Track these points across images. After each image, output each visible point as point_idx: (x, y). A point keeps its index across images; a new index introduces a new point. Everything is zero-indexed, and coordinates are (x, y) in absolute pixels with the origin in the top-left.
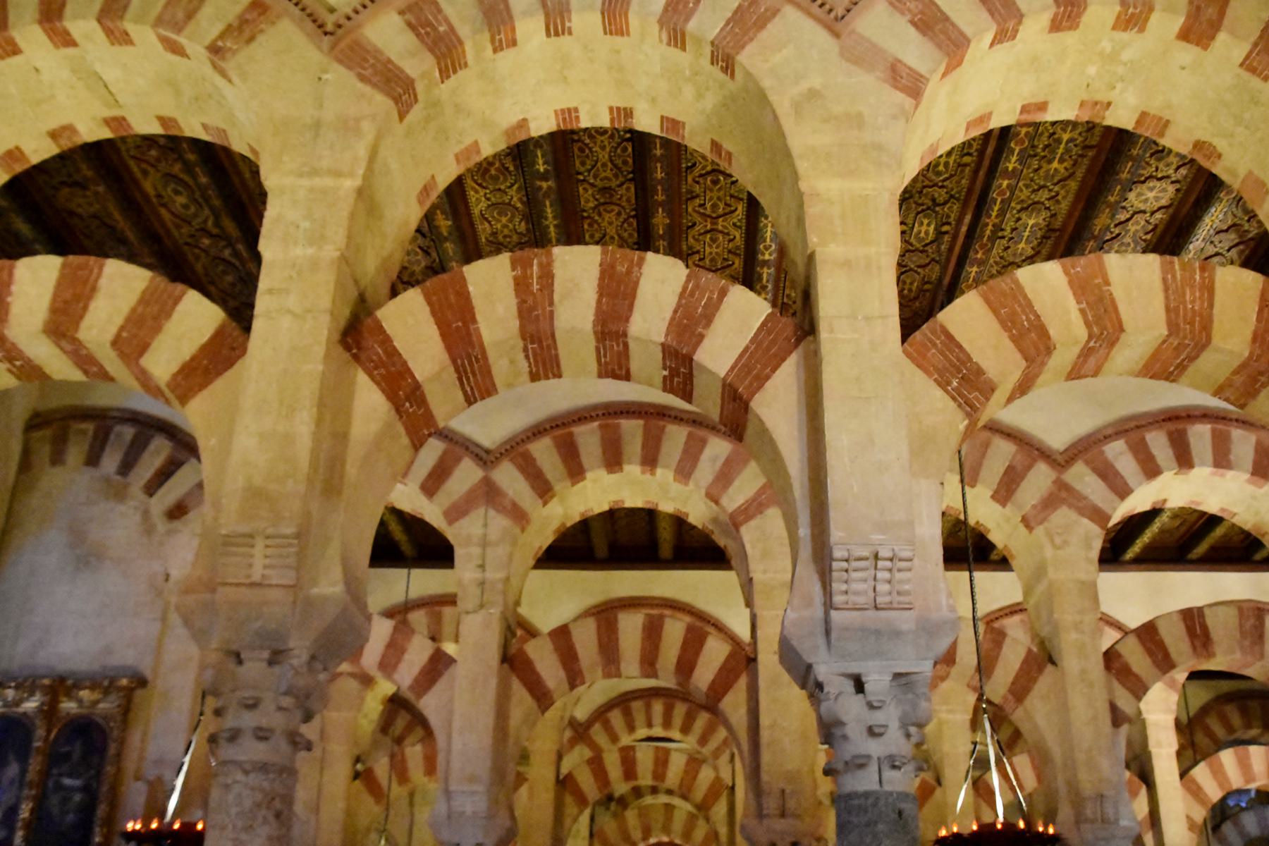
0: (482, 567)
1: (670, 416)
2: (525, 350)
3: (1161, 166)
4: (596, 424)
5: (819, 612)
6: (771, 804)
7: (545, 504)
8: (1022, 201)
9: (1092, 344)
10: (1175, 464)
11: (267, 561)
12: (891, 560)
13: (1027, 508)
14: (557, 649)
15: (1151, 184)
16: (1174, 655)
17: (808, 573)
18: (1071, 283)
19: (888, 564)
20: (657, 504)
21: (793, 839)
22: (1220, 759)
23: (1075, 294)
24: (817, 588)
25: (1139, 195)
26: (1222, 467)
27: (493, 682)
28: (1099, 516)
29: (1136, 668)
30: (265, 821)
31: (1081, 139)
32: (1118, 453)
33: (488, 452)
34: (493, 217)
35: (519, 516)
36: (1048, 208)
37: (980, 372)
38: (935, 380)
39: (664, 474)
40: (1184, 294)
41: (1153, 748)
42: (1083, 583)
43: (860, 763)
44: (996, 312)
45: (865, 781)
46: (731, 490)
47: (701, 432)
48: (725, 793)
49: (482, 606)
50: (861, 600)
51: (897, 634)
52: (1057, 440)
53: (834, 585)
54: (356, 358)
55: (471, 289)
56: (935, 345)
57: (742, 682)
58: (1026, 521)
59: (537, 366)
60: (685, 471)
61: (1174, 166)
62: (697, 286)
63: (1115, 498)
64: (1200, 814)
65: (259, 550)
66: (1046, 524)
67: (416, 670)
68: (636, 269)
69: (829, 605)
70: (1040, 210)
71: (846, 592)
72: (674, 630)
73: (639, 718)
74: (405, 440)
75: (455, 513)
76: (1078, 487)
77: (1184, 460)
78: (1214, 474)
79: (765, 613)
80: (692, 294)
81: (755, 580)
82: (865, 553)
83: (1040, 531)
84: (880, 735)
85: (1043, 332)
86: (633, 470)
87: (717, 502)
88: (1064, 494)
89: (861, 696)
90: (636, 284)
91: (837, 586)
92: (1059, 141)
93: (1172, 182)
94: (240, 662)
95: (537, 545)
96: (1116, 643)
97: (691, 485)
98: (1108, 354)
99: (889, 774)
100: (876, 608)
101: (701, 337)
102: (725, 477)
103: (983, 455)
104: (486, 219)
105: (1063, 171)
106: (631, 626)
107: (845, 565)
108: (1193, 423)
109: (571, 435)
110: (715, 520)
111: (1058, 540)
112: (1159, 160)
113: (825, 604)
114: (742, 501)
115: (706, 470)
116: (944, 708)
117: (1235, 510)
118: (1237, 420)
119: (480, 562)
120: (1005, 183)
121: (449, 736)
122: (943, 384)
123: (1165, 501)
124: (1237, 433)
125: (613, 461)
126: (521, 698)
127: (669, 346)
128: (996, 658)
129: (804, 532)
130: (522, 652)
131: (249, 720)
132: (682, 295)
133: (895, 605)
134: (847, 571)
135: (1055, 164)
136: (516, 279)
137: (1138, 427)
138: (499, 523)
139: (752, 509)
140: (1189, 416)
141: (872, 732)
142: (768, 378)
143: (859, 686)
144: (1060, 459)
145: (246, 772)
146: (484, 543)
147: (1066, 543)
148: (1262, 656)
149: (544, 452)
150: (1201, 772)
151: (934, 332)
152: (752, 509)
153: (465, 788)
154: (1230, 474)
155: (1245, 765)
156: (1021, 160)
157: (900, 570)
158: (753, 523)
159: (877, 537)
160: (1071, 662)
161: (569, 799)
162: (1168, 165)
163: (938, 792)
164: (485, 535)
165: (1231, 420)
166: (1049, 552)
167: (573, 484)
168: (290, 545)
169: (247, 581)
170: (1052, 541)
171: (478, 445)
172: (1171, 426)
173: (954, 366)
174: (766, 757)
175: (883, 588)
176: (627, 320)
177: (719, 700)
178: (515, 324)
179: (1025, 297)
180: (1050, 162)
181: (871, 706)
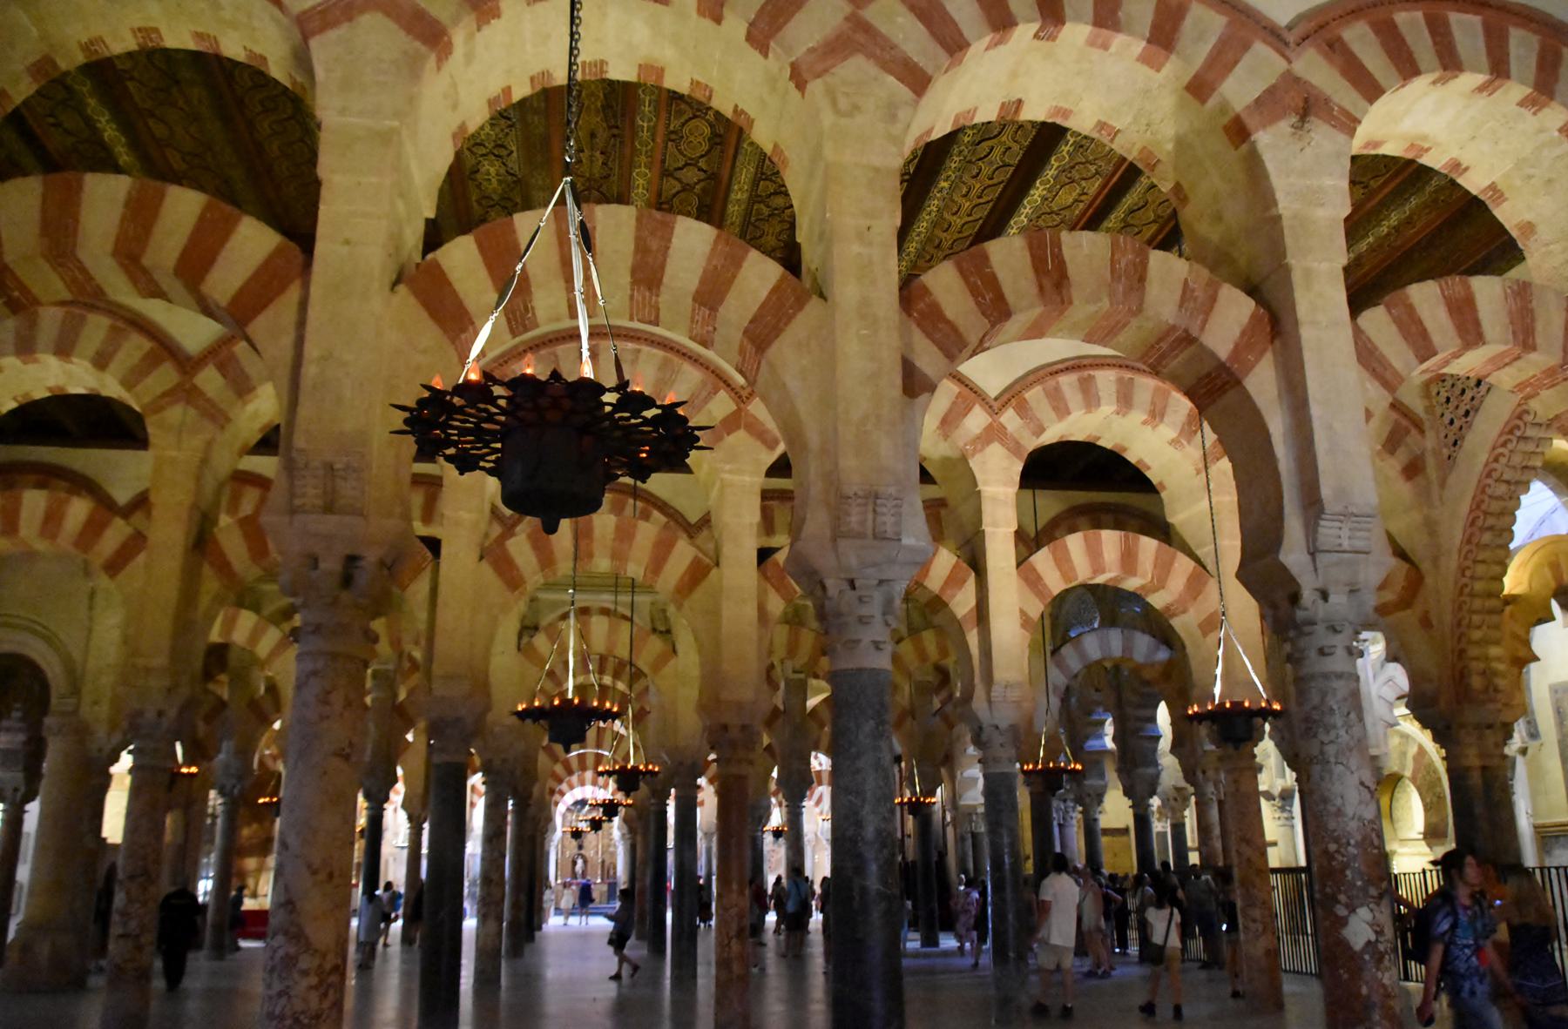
10: (1038, 15)
13: (800, 51)
21: (348, 552)
22: (1066, 546)
26: (1107, 27)
29: (950, 313)
42: (877, 170)
57: (293, 294)
58: (799, 78)
64: (1036, 609)
66: (828, 78)
76: (883, 28)
79: (337, 178)
88: (860, 37)
111: (843, 103)
116: (728, 467)
117: (1117, 125)
128: (730, 281)
147: (856, 108)
148: (1140, 310)
150: (1042, 559)
154: (1119, 40)
155: (1094, 553)
158: (332, 34)
163: (714, 572)
166: (828, 118)
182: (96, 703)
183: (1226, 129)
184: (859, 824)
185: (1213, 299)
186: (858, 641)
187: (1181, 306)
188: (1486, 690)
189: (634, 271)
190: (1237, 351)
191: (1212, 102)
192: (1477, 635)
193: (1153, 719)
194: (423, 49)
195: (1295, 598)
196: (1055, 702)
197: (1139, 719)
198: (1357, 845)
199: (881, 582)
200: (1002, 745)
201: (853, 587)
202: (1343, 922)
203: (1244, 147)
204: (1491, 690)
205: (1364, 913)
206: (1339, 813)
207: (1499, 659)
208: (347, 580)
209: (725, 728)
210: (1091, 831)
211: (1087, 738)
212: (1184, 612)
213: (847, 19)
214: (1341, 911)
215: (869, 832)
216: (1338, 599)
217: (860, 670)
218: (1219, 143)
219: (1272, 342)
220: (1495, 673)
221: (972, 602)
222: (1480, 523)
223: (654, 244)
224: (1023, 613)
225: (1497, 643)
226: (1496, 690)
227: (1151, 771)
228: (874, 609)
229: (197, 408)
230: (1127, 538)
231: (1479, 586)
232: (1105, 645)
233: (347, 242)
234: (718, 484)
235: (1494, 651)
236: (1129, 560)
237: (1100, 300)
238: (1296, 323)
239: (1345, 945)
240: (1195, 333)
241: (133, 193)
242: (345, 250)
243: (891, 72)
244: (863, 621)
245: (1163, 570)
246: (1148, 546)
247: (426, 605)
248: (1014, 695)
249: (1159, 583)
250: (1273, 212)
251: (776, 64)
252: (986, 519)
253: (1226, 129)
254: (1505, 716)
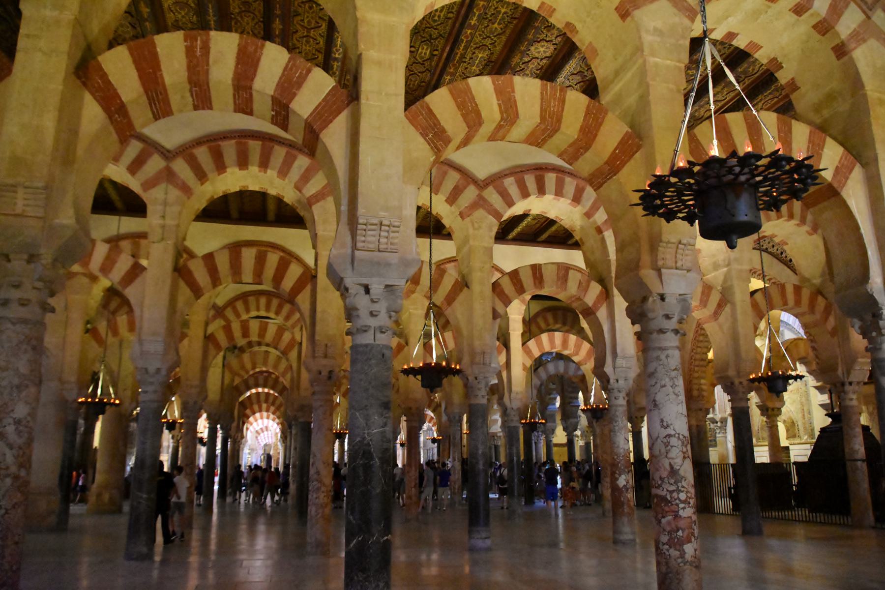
0: (163, 217)
1: (277, 141)
2: (191, 91)
3: (549, 34)
4: (233, 141)
5: (349, 251)
6: (320, 352)
7: (202, 184)
8: (477, 43)
9: (502, 123)
11: (26, 202)
12: (389, 226)
15: (543, 44)
16: (525, 286)
17: (345, 230)
18: (495, 89)
19: (387, 228)
20: (267, 190)
23: (496, 95)
24: (349, 239)
25: (536, 48)
27: (169, 282)
28: (497, 215)
29: (507, 292)
30: (26, 351)
31: (510, 13)
32: (510, 184)
33: (168, 151)
34: (177, 10)
35: (186, 189)
36: (489, 49)
37: (444, 131)
38: (421, 133)
39: (272, 173)
40: (550, 102)
41: (511, 332)
43: (365, 330)
44: (456, 101)
45: (367, 339)
46: (308, 185)
47: (295, 152)
49: (163, 239)
50: (371, 246)
51: (388, 265)
52: (481, 173)
53: (358, 237)
54: (84, 84)
55: (158, 50)
56: (422, 115)
57: (309, 288)
58: (462, 215)
59: (197, 101)
60: (283, 172)
61: (555, 36)
62: (294, 65)
63: (507, 207)
64: (529, 363)
65: (21, 193)
66: (471, 217)
67: (123, 273)
68: (259, 50)
69: (354, 247)
70: (485, 50)
71: (364, 242)
72: (273, 259)
73: (253, 306)
74: (114, 137)
75: (148, 185)
76: (489, 199)
77: (541, 191)
78: (554, 199)
80: (291, 69)
81: (318, 234)
82: (375, 221)
83: (468, 220)
84: (376, 316)
85: (478, 114)
86: (254, 169)
87: (300, 191)
88: (481, 202)
89: (368, 295)
90: (259, 60)
91: (359, 238)
92: (499, 12)
93: (553, 44)
94: (9, 261)
95: (196, 207)
96: (499, 279)
97: (287, 180)
98: (510, 130)
99: (379, 336)
100: (379, 251)
101: (295, 95)
102: (306, 177)
103: (444, 178)
104: (172, 11)
105: (499, 29)
106: (248, 256)
107: (364, 227)
108: (548, 172)
109: (219, 146)
110: (299, 201)
111: (476, 225)
112: (548, 31)
113: (352, 247)
114: (314, 192)
115: (296, 172)
117: (562, 218)
118: (569, 173)
120: (469, 31)
121: (142, 311)
122: (424, 135)
123: (530, 210)
124: (568, 179)
125: (243, 162)
126: (185, 291)
127: (276, 98)
129: (344, 208)
130: (185, 266)
131: (15, 294)
132: (285, 69)
133: (389, 250)
134: (365, 230)
135: (496, 25)
136: (186, 47)
137: (521, 171)
138: (174, 193)
139: (319, 197)
140: (546, 168)
141: (372, 314)
142: (331, 121)
143: (367, 290)
144: (481, 184)
145: (14, 324)
146: (165, 204)
147: (480, 227)
148: (565, 289)
149: (202, 154)
150: (532, 344)
151: (422, 107)
152: (319, 197)
154: (562, 199)
155: (552, 341)
156: (478, 20)
157: (393, 232)
158: (319, 204)
159: (382, 214)
160: (476, 287)
161: (211, 347)
162: (552, 35)
163: (406, 348)
164: (166, 199)
165: (566, 172)
166: (471, 231)
167: (219, 175)
168: (41, 193)
169: (13, 213)
170: (473, 225)
171: (163, 147)
172: (538, 173)
173: (430, 126)
175: (383, 240)
176: (252, 80)
177: (296, 297)
178: (184, 74)
179: (471, 93)
180: (493, 24)
181: (372, 301)
182: (125, 390)
183: (596, 228)
184: (477, 450)
185: (588, 286)
186: (478, 395)
187: (578, 288)
188: (699, 396)
190: (595, 304)
191: (591, 220)
192: (696, 375)
193: (577, 398)
195: (608, 381)
196: (535, 392)
197: (571, 398)
198: (623, 456)
199: (485, 377)
200: (514, 415)
201: (476, 378)
202: (617, 479)
203: (601, 236)
204: (701, 397)
205: (623, 477)
206: (618, 447)
207: (705, 384)
208: (330, 378)
209: (410, 408)
210: (549, 446)
211: (548, 404)
212: (586, 364)
213: (477, 196)
214: (617, 476)
215: (480, 452)
216: (621, 382)
217: (478, 404)
218: (594, 232)
219: (606, 300)
220: (702, 390)
221: (505, 360)
222: (699, 332)
224: (523, 364)
225: (703, 378)
226: (703, 396)
227: (575, 420)
228: (482, 386)
230: (564, 335)
231: (698, 356)
232: (556, 367)
234: (407, 313)
235: (703, 381)
236: (565, 343)
237: (553, 287)
238: (613, 296)
239: (617, 485)
240: (582, 297)
243: (491, 215)
244: (479, 389)
245: (578, 347)
246: (573, 338)
247: (296, 361)
248: (519, 396)
249: (577, 353)
250: (608, 258)
251: (455, 209)
252: (511, 328)
253: (596, 228)
254: (707, 406)
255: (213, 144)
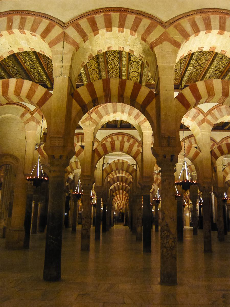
0: (62, 61)
4: (103, 14)
14: (89, 90)
48: (140, 154)
87: (145, 41)
102: (148, 31)
119: (61, 60)
138: (68, 47)
139: (159, 41)
149: (84, 23)
152: (159, 41)
153: (56, 136)
158: (158, 47)
174: (163, 126)
189: (222, 93)
194: (177, 48)
223: (226, 87)
229: (92, 121)
233: (166, 90)
241: (120, 82)
242: (166, 92)
255: (89, 17)
